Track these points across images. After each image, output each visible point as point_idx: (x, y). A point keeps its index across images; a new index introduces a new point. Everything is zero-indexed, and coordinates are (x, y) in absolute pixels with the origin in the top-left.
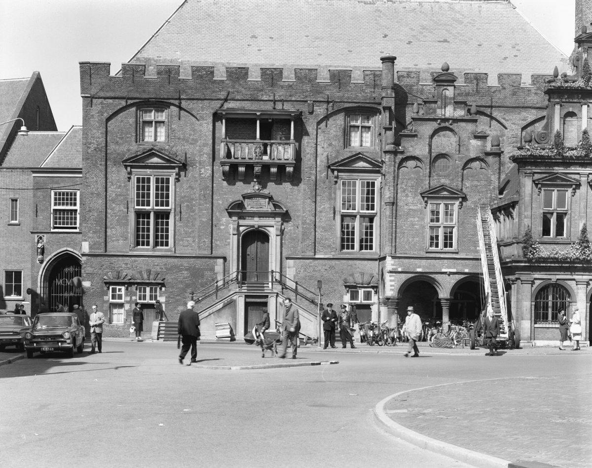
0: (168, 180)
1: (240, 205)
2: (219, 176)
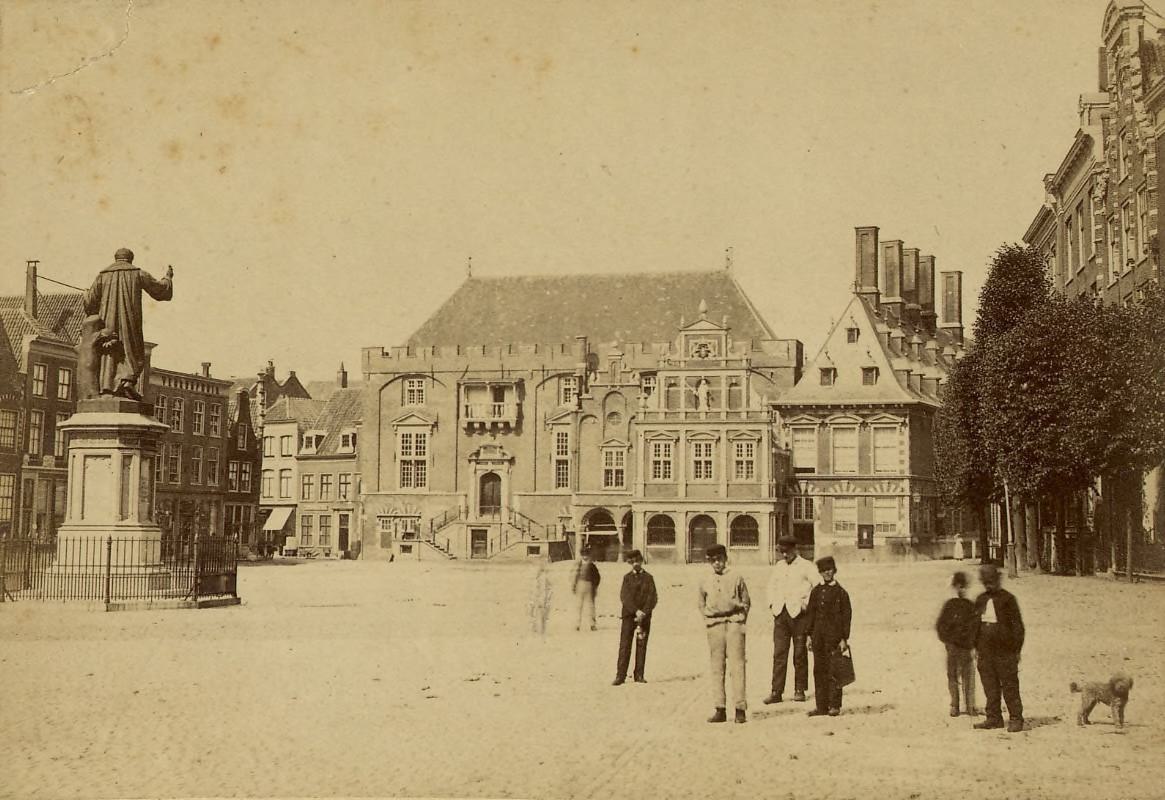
0: (424, 435)
1: (477, 453)
2: (462, 433)
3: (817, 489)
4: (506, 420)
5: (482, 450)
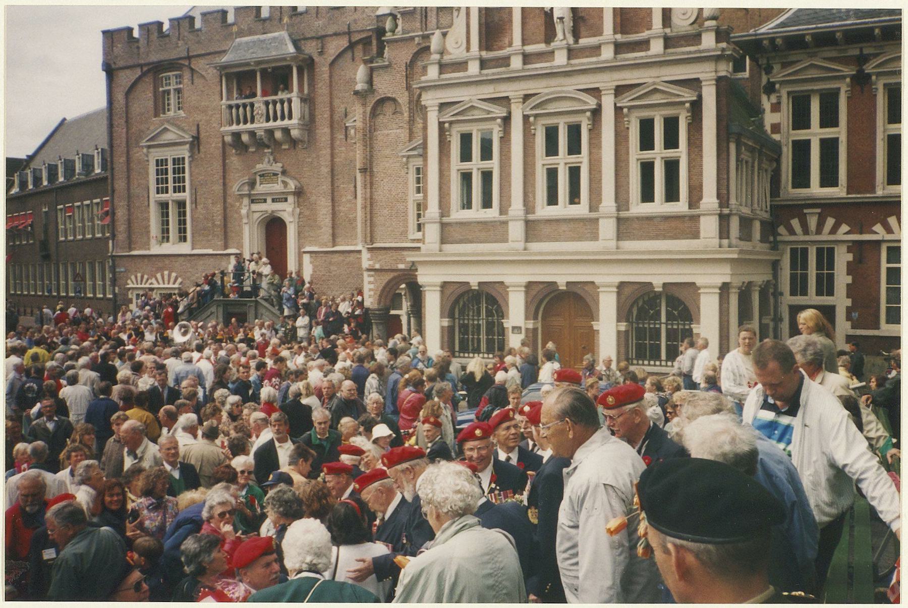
3: (845, 228)
4: (286, 122)
5: (258, 178)
